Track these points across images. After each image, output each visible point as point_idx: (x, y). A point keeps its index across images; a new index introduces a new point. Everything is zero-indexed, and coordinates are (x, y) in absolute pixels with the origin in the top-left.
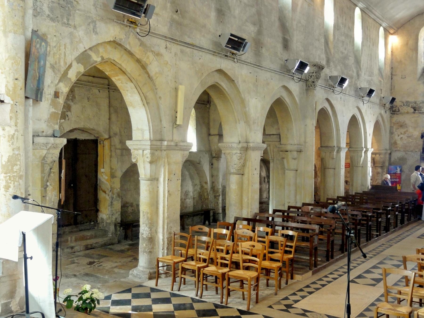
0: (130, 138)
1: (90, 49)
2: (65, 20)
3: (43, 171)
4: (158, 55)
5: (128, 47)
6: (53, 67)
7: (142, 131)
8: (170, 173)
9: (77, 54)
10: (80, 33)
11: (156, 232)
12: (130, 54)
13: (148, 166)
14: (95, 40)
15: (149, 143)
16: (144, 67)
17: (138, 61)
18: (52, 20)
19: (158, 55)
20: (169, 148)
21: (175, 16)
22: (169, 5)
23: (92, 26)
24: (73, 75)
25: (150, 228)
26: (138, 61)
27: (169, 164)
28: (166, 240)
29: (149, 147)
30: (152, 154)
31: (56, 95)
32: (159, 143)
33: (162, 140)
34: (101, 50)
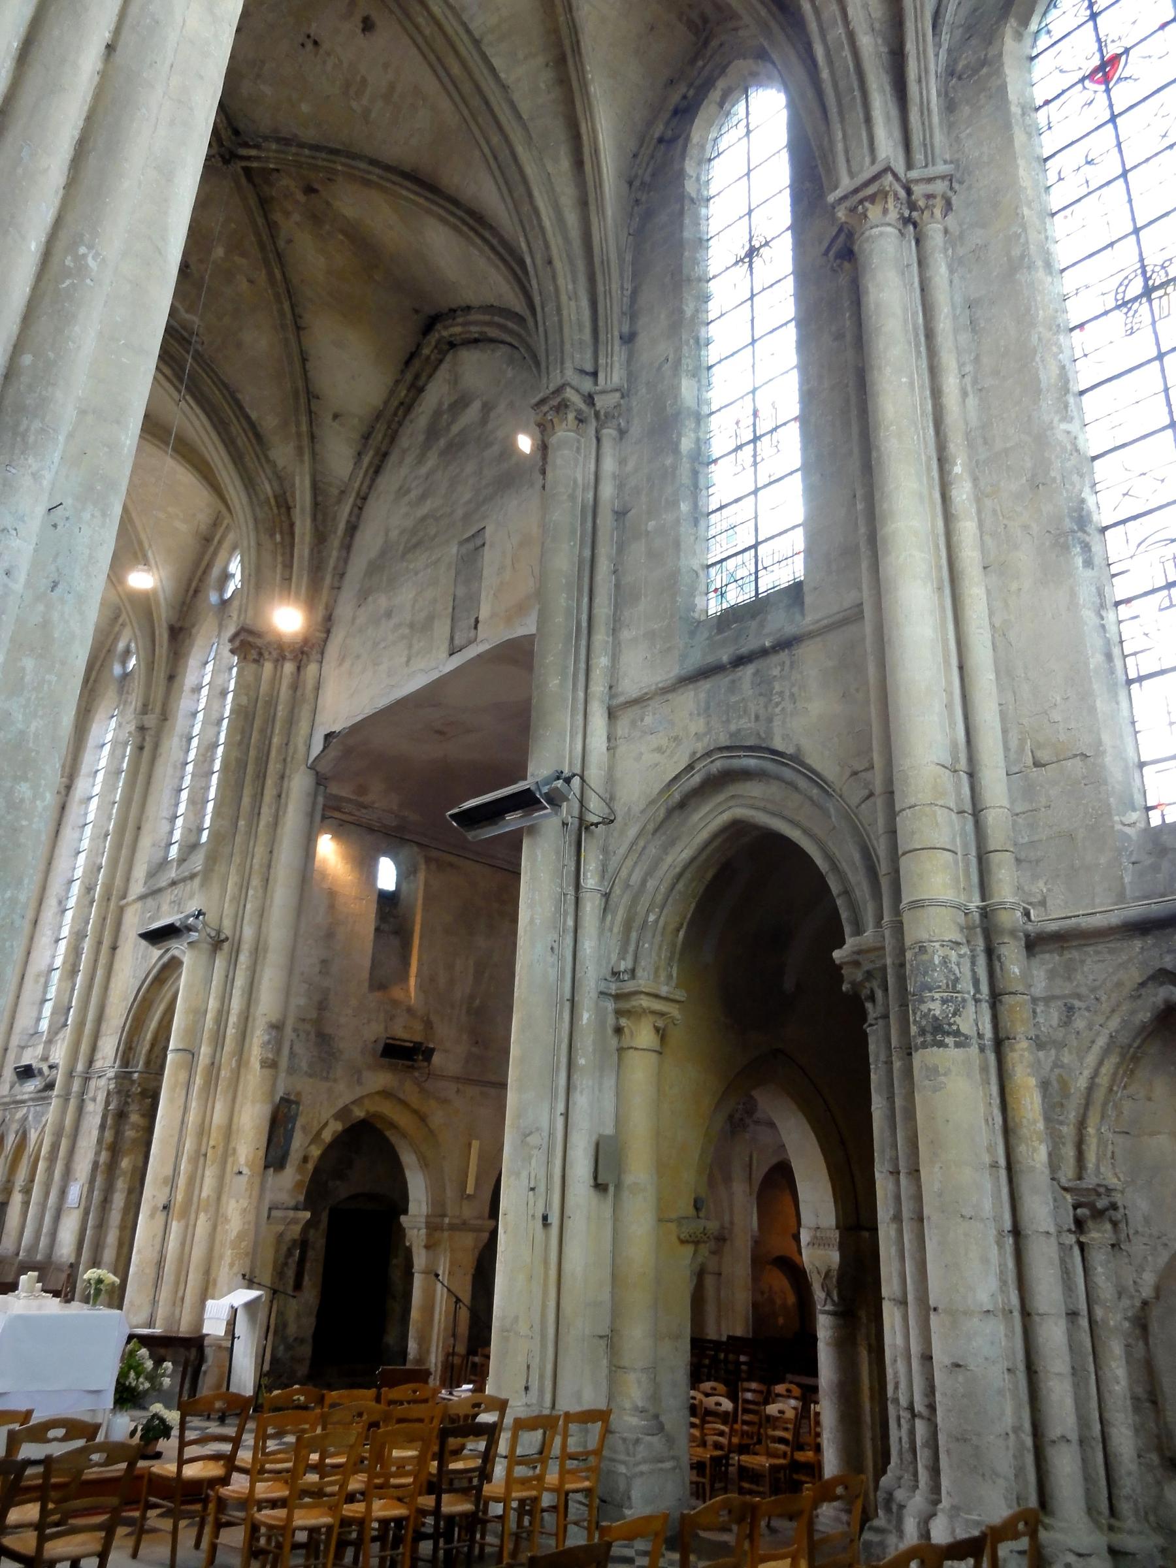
0: (405, 1211)
1: (353, 1103)
2: (325, 1074)
3: (277, 1251)
4: (445, 1101)
5: (401, 1096)
6: (304, 1128)
7: (420, 1202)
8: (452, 1264)
9: (333, 1111)
10: (341, 1087)
11: (428, 1352)
12: (404, 1103)
13: (423, 1252)
14: (359, 1092)
15: (423, 1220)
16: (422, 1118)
17: (415, 1112)
18: (310, 1076)
19: (445, 1101)
20: (453, 1227)
21: (474, 1049)
22: (465, 1037)
23: (356, 1077)
24: (327, 1136)
25: (420, 1345)
26: (415, 1112)
27: (452, 1251)
28: (439, 1365)
29: (423, 1225)
30: (429, 1235)
31: (305, 1159)
32: (438, 1220)
33: (444, 1215)
34: (366, 1101)
